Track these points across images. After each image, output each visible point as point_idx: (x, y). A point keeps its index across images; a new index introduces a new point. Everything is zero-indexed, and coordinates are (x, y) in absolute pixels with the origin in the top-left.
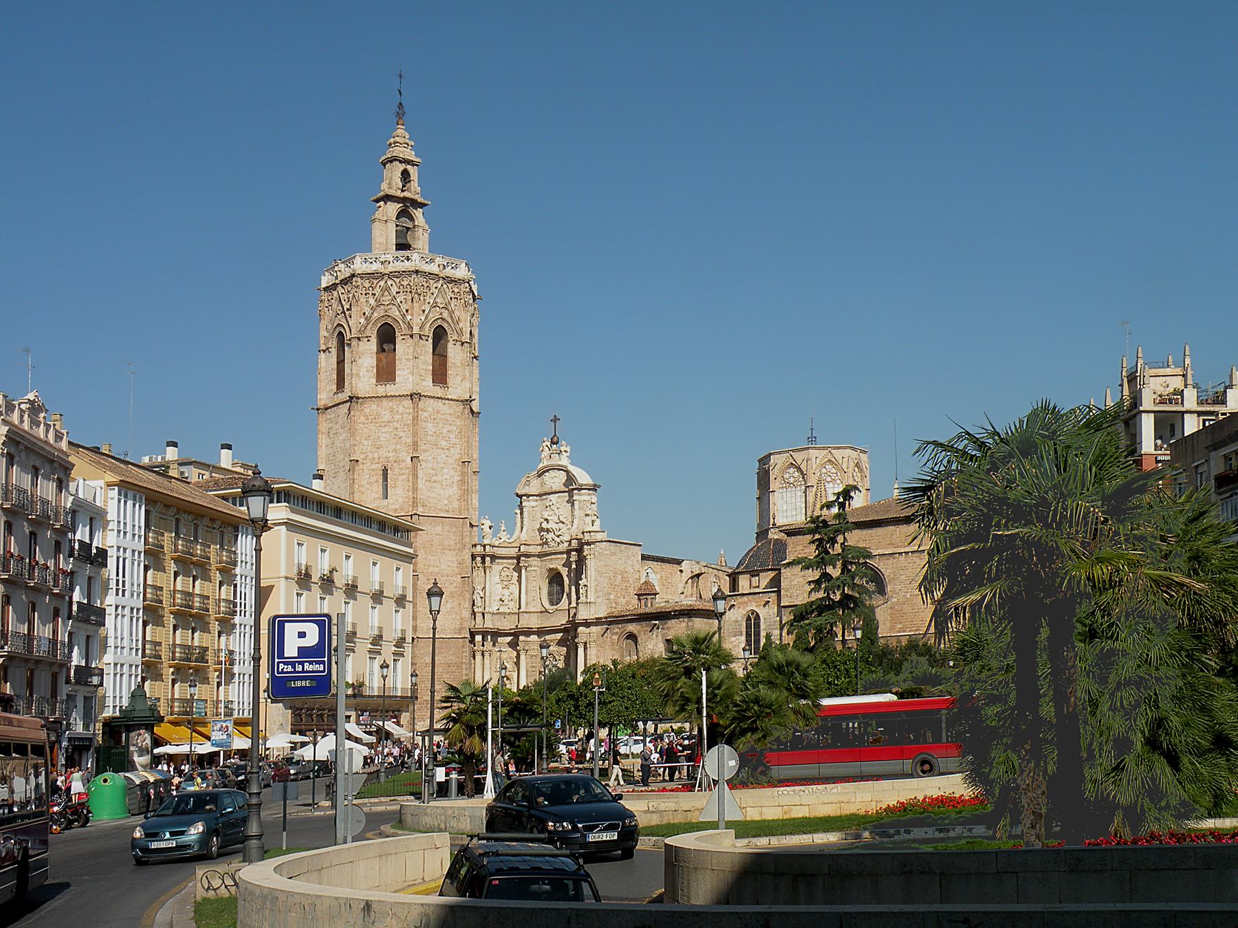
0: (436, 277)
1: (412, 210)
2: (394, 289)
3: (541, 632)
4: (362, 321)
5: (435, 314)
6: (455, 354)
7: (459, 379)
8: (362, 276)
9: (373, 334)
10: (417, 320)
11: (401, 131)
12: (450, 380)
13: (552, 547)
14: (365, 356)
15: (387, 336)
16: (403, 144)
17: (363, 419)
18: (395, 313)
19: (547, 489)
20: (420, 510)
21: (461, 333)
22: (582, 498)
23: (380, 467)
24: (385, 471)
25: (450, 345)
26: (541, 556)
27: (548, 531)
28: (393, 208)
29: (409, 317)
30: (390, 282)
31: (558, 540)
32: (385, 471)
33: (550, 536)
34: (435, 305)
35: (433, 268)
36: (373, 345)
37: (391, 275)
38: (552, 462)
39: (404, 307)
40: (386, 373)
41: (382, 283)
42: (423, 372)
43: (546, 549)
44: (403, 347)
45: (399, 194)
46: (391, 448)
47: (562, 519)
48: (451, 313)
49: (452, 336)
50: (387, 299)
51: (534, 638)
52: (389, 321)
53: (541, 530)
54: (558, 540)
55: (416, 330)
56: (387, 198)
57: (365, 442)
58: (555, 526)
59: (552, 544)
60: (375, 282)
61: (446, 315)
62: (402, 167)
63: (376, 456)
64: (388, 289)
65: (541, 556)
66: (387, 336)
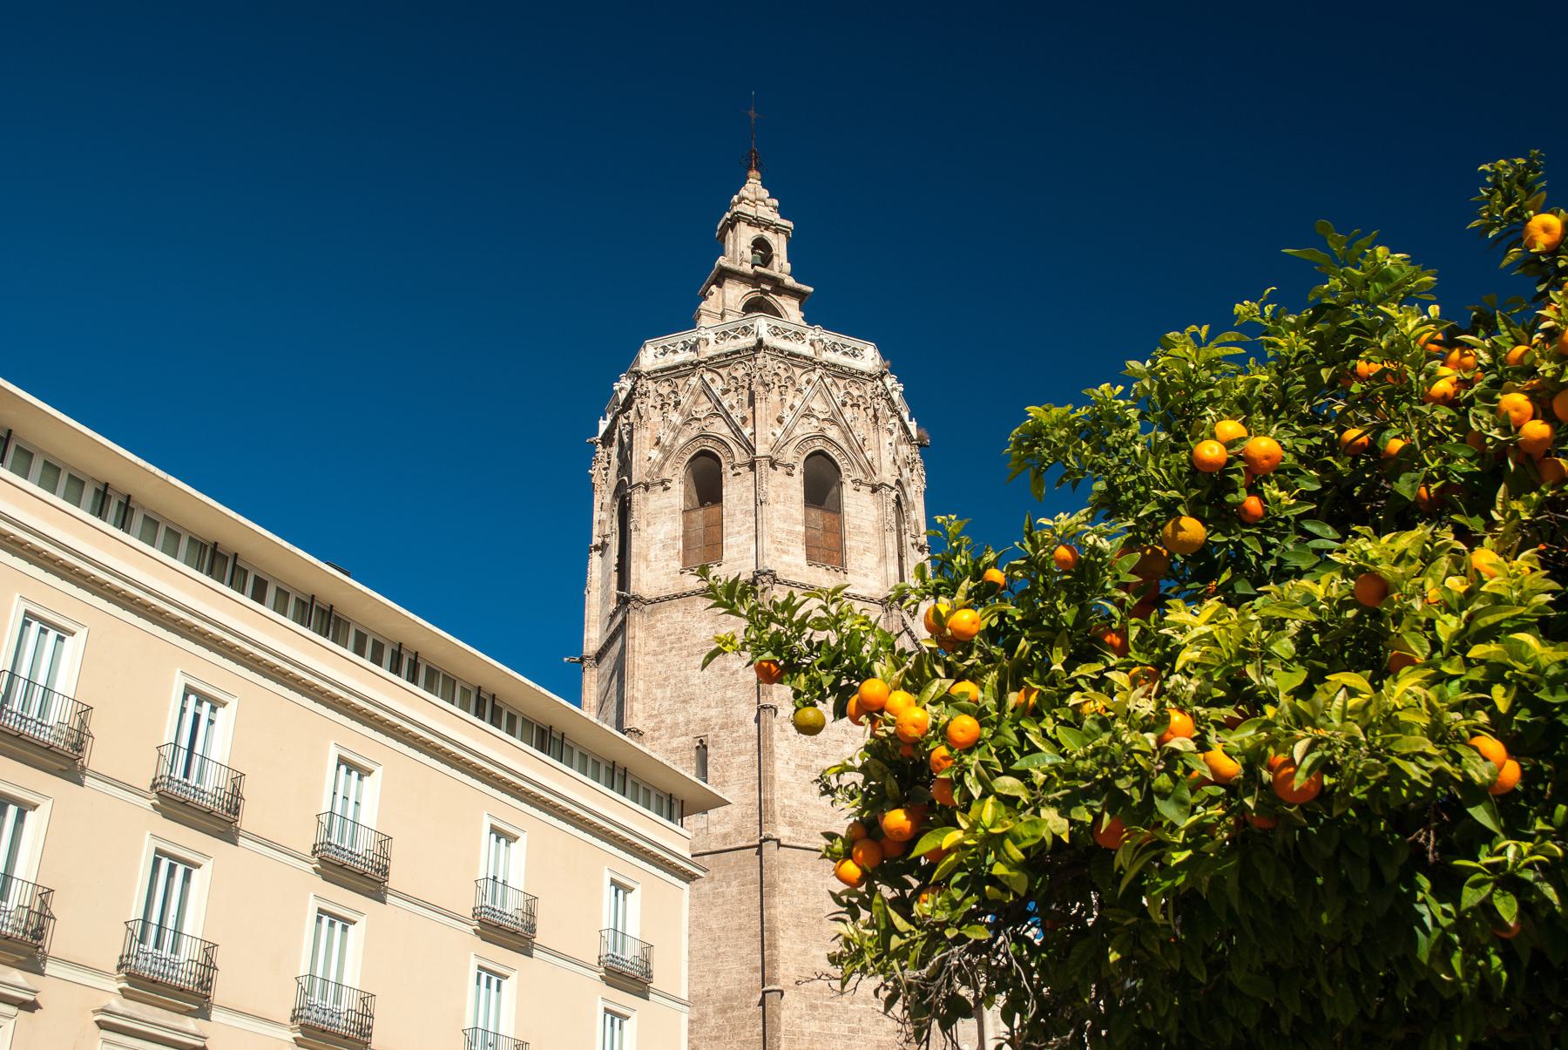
0: (810, 363)
1: (773, 299)
2: (717, 387)
4: (656, 454)
5: (805, 428)
6: (860, 509)
7: (871, 560)
8: (658, 375)
9: (677, 476)
10: (765, 437)
11: (753, 188)
12: (852, 560)
14: (662, 519)
15: (706, 482)
16: (755, 198)
17: (653, 644)
18: (720, 428)
20: (783, 832)
21: (870, 469)
23: (689, 741)
24: (702, 749)
25: (848, 490)
28: (735, 294)
29: (747, 431)
30: (708, 376)
32: (702, 749)
34: (809, 414)
35: (804, 349)
36: (677, 495)
37: (714, 364)
39: (736, 415)
40: (703, 547)
41: (694, 380)
42: (782, 536)
44: (735, 490)
45: (747, 268)
46: (714, 697)
48: (847, 431)
49: (849, 474)
50: (705, 406)
52: (710, 445)
55: (762, 449)
56: (725, 275)
57: (658, 693)
60: (680, 382)
61: (833, 433)
62: (754, 233)
63: (681, 718)
64: (706, 389)
66: (706, 482)
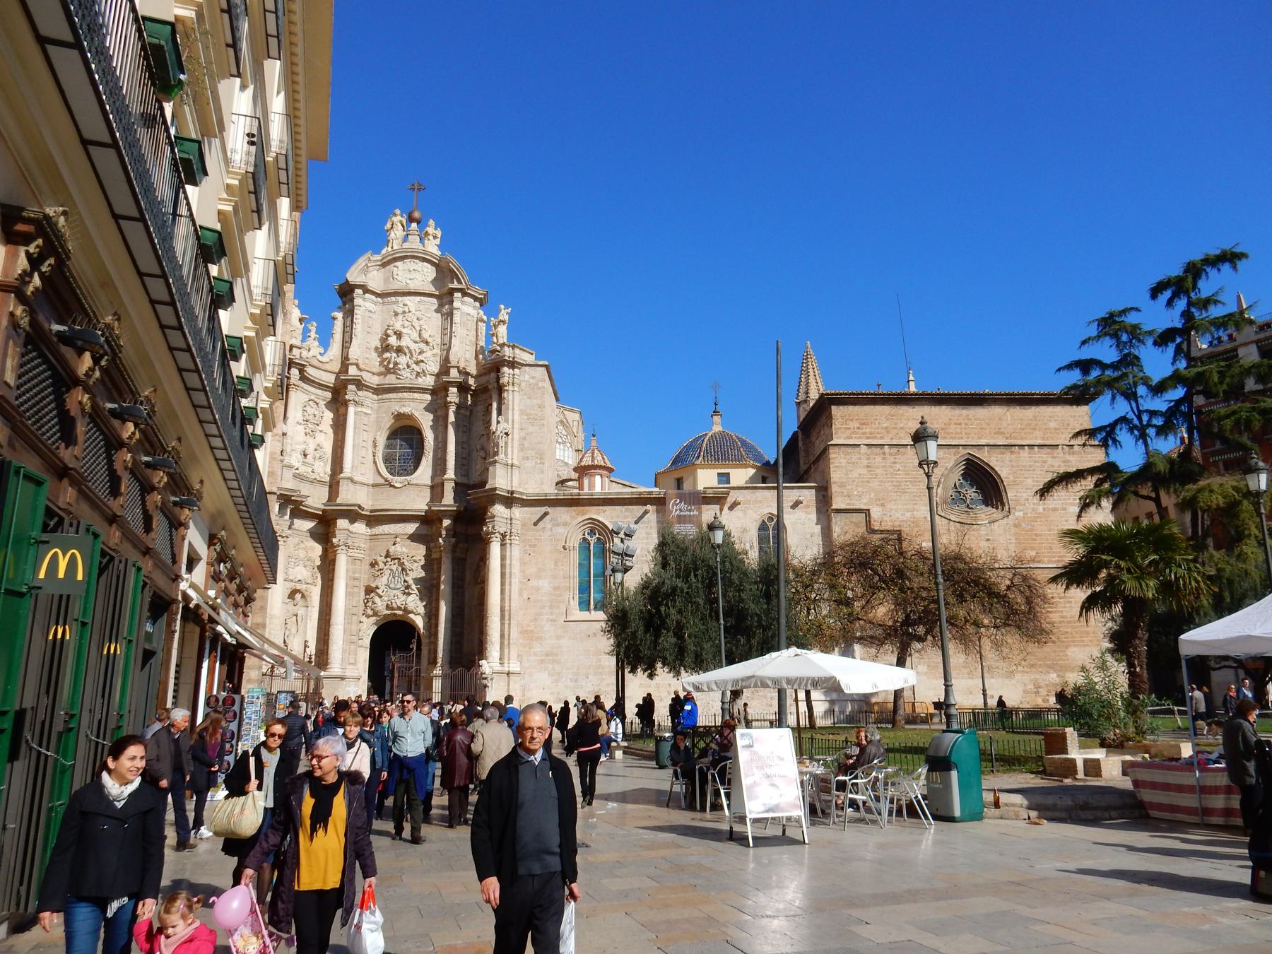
3: (375, 519)
13: (407, 377)
19: (395, 286)
22: (466, 309)
26: (379, 391)
27: (399, 350)
31: (417, 368)
33: (403, 360)
38: (406, 245)
43: (391, 379)
47: (425, 335)
51: (360, 527)
53: (386, 348)
54: (417, 368)
58: (413, 346)
59: (406, 374)
65: (379, 391)
